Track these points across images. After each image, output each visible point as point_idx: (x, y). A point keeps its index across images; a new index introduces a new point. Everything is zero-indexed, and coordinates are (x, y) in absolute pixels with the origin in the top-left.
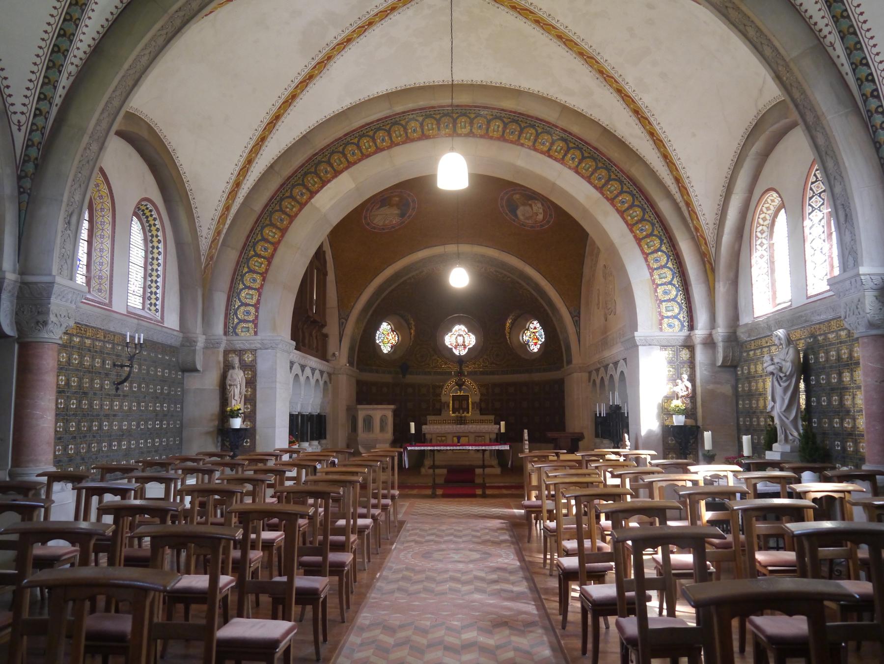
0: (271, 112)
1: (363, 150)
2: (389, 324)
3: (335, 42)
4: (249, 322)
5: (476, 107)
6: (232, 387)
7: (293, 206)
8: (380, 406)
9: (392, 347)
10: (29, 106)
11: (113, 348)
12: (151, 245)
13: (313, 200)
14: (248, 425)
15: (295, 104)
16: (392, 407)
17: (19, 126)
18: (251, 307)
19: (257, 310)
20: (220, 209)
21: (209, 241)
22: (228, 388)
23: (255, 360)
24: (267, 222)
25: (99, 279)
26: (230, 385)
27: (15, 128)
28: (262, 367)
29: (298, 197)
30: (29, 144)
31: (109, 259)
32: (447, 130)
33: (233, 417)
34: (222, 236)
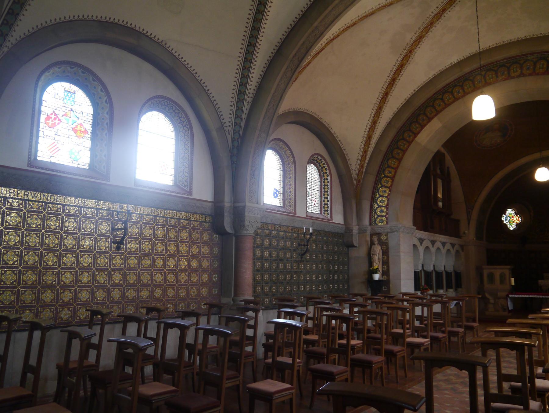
0: (382, 92)
1: (446, 102)
2: (513, 210)
3: (412, 41)
4: (383, 216)
5: (523, 55)
6: (374, 255)
7: (405, 144)
8: (498, 267)
9: (516, 225)
10: (232, 122)
11: (298, 236)
12: (323, 178)
13: (416, 139)
14: (385, 278)
15: (396, 83)
16: (509, 267)
17: (229, 132)
18: (384, 208)
19: (387, 209)
20: (361, 152)
21: (357, 171)
22: (372, 256)
23: (387, 239)
24: (390, 156)
25: (289, 200)
26: (373, 254)
27: (227, 133)
28: (391, 243)
29: (407, 138)
30: (233, 140)
31: (293, 189)
32: (503, 76)
33: (374, 273)
34: (365, 168)
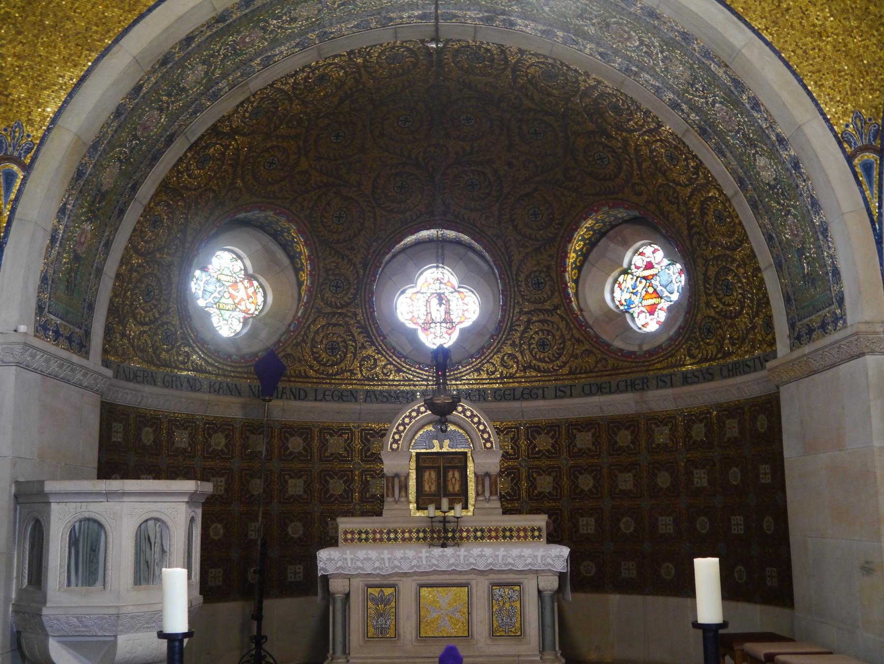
8: (131, 485)
9: (245, 322)
16: (189, 486)
